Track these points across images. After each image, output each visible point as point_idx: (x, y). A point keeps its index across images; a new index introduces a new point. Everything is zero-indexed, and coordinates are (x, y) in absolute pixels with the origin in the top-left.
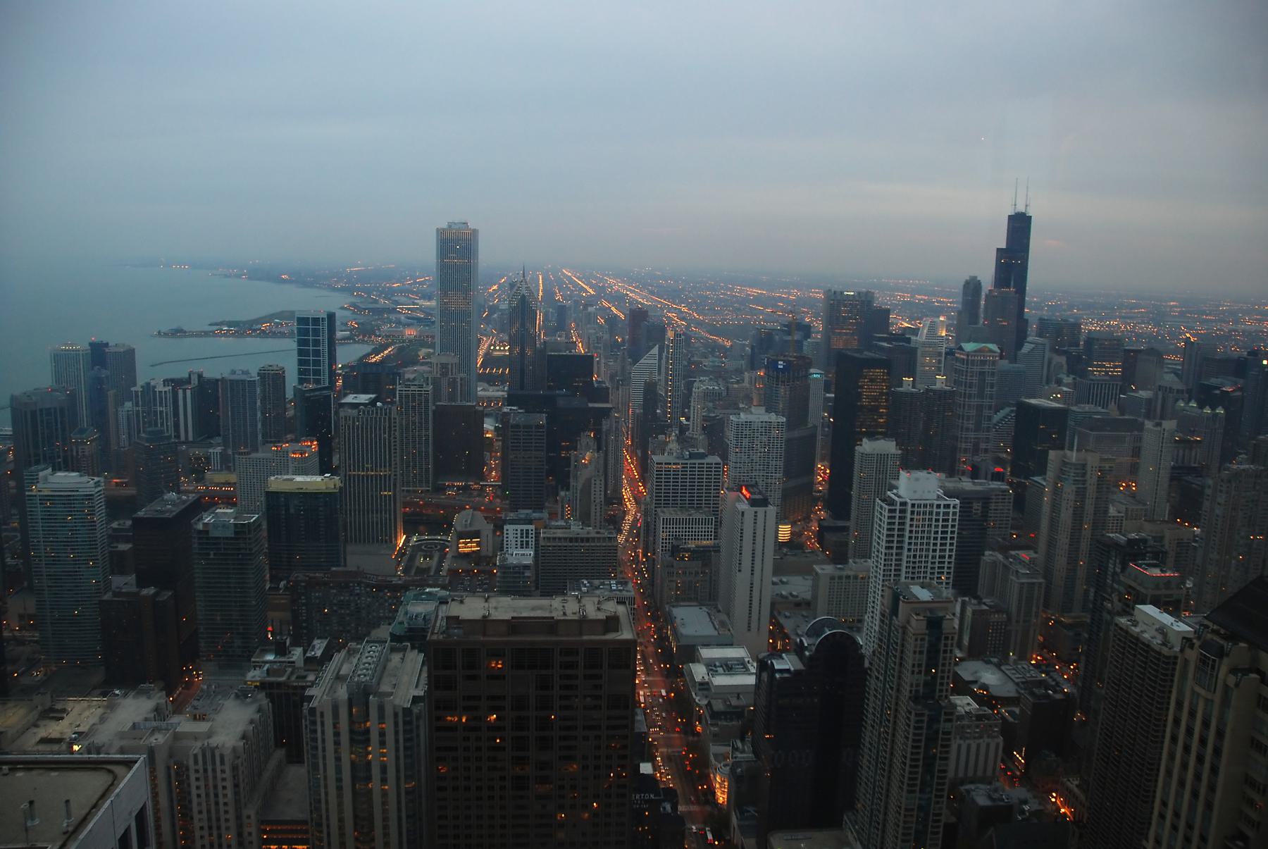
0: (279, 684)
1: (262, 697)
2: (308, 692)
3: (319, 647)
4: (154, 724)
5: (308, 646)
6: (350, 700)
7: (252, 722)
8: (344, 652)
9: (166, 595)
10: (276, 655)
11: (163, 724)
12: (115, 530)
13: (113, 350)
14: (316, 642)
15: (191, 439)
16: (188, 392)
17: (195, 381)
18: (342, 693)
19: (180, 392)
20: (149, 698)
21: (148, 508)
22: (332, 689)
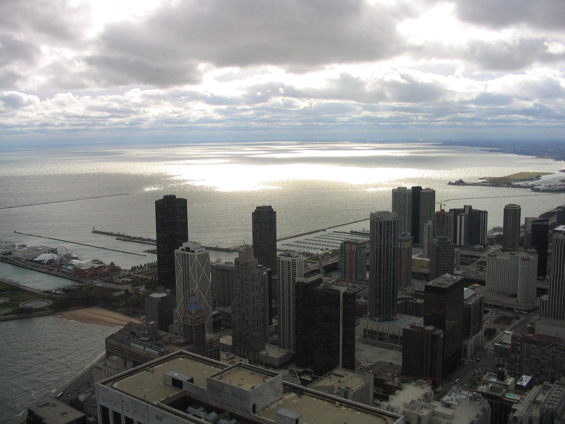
0: (497, 398)
1: (486, 404)
2: (514, 407)
3: (525, 380)
4: (423, 403)
5: (518, 377)
6: (541, 419)
7: (478, 416)
8: (540, 387)
9: (439, 332)
10: (498, 379)
11: (427, 404)
12: (416, 291)
13: (423, 191)
14: (524, 377)
15: (462, 244)
16: (463, 217)
17: (467, 212)
18: (536, 413)
19: (459, 217)
20: (422, 388)
21: (435, 280)
22: (529, 409)
